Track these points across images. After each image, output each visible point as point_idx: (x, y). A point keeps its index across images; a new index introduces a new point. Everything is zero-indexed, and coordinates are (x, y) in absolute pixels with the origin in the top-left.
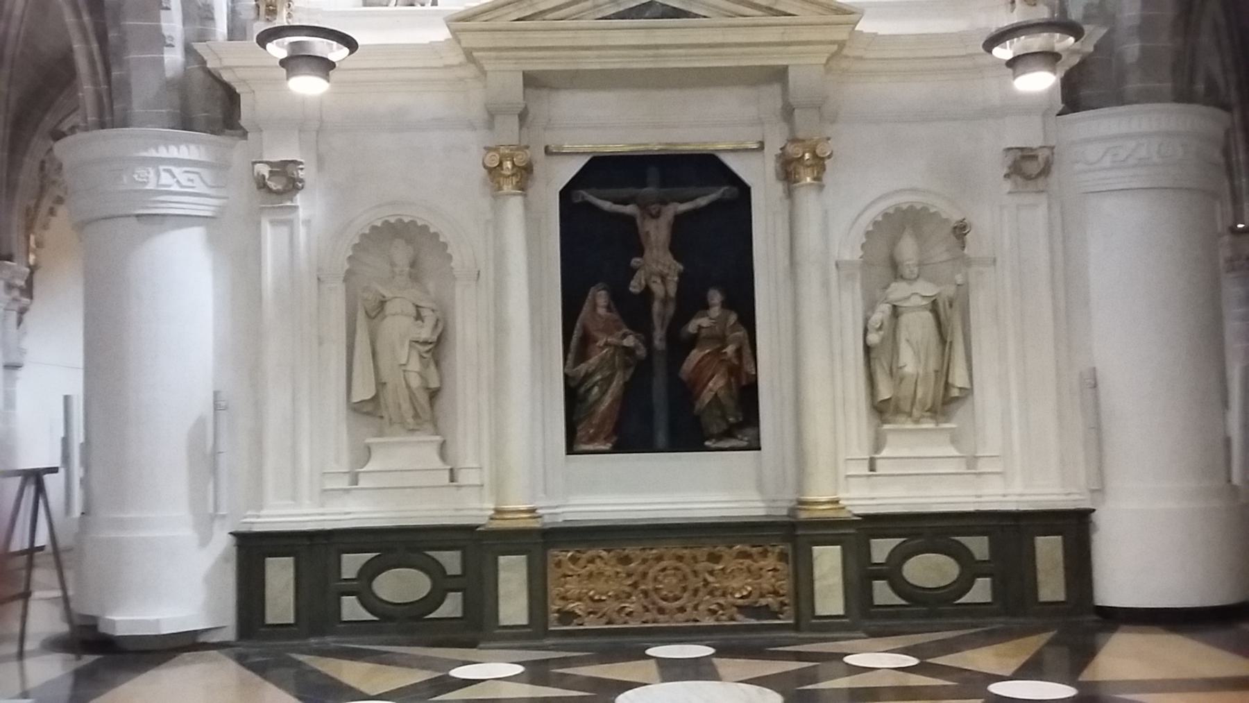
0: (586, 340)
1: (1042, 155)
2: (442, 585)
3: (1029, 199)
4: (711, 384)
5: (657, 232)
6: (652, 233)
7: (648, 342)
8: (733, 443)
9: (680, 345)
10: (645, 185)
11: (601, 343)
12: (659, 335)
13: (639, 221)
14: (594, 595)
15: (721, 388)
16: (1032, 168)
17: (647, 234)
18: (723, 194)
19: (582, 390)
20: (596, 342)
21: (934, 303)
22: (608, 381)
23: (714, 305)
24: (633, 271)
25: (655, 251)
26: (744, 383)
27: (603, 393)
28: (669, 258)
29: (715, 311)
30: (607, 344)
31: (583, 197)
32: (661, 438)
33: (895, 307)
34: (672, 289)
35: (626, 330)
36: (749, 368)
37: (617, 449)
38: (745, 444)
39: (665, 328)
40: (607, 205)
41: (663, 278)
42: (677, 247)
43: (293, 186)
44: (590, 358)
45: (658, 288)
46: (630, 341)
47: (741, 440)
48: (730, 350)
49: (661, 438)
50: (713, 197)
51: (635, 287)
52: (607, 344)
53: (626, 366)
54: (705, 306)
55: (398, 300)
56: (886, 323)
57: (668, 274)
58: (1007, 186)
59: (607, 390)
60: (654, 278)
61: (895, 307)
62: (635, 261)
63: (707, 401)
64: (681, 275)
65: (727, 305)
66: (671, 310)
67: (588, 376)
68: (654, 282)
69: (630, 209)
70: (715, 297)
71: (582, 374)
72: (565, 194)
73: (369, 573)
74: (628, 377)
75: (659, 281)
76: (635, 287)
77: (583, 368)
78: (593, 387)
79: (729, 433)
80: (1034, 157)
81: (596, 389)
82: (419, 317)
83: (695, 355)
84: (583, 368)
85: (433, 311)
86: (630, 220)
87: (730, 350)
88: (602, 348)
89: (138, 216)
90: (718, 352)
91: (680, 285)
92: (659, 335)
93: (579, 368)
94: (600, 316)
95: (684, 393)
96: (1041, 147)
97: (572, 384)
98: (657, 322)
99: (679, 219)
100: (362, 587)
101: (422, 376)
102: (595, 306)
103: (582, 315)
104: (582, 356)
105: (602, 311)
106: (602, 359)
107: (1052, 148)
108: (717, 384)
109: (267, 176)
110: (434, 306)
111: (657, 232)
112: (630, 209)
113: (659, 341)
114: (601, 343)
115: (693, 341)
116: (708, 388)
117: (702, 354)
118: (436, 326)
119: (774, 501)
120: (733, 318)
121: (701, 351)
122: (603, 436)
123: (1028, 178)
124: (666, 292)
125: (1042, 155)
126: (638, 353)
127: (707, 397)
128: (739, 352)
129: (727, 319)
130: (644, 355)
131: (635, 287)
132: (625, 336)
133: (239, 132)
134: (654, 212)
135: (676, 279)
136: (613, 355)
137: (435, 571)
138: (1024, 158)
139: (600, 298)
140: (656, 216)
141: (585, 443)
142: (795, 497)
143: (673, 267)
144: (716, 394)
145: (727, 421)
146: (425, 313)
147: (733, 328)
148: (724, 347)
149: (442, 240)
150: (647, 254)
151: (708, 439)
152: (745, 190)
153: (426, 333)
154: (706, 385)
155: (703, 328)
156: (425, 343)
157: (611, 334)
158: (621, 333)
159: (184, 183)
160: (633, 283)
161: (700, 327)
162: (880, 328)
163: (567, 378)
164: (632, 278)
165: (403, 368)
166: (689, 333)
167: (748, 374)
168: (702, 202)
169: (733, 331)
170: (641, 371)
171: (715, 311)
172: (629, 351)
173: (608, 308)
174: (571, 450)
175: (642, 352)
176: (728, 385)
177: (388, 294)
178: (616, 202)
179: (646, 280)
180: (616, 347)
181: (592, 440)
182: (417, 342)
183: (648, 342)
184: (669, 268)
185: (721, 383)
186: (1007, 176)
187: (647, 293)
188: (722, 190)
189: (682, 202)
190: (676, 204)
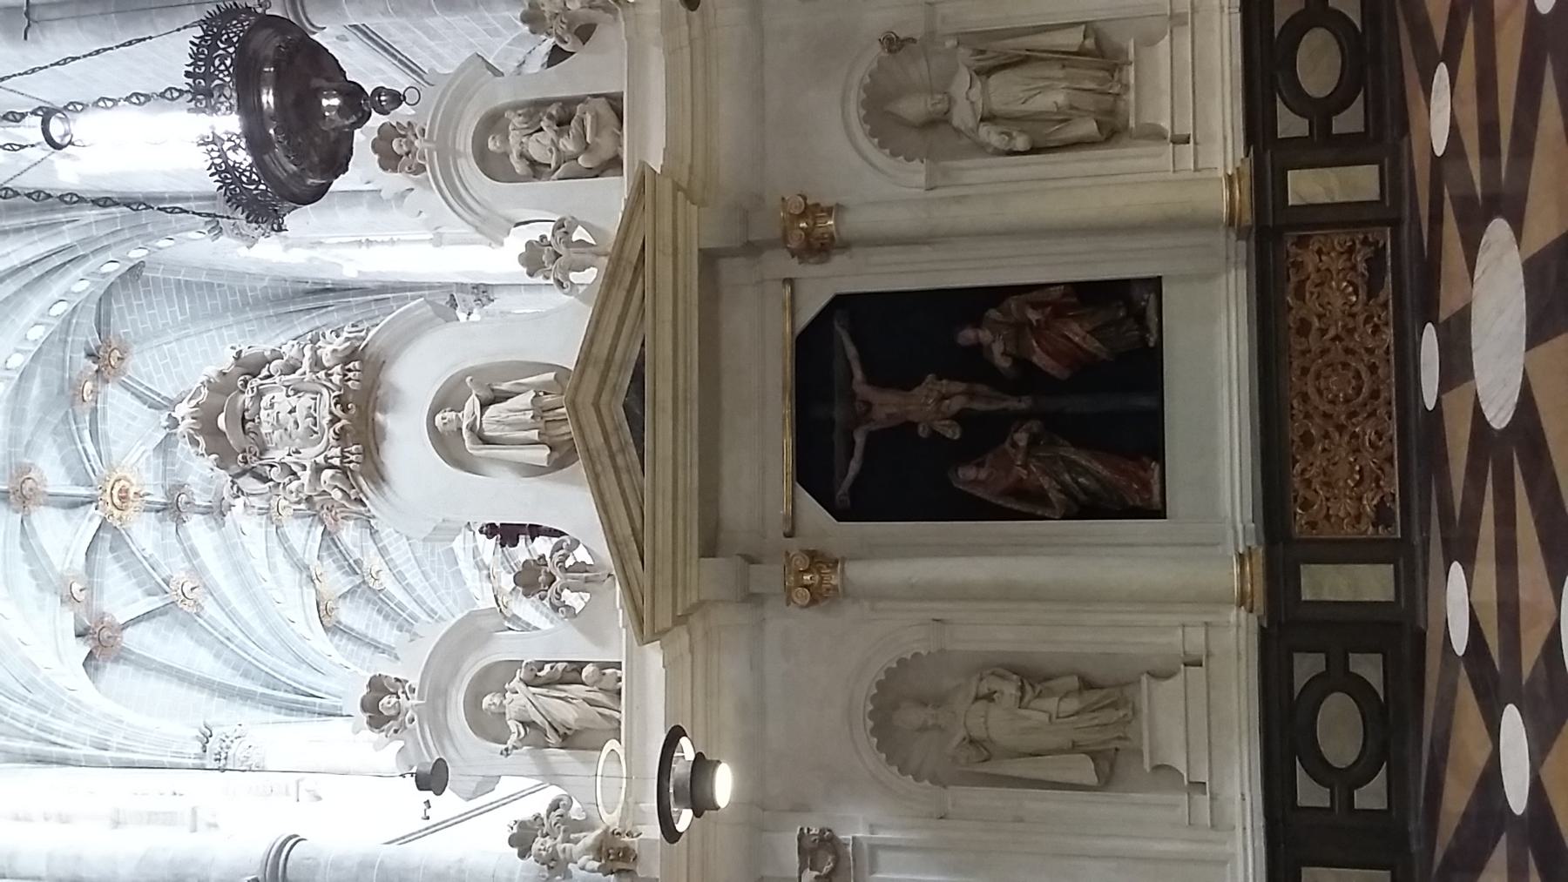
4: (1077, 339)
5: (887, 405)
9: (1026, 377)
14: (1353, 480)
15: (1081, 326)
17: (889, 416)
18: (843, 327)
19: (1082, 497)
22: (1071, 466)
24: (935, 434)
27: (1086, 472)
30: (1025, 466)
31: (845, 495)
34: (959, 386)
40: (854, 466)
42: (906, 382)
44: (1041, 487)
45: (956, 404)
46: (1022, 438)
47: (1147, 301)
48: (1033, 316)
59: (1082, 466)
60: (943, 408)
62: (922, 432)
63: (1097, 344)
66: (982, 388)
67: (1064, 489)
69: (860, 439)
71: (1063, 497)
76: (953, 433)
78: (1077, 483)
81: (1081, 480)
82: (989, 697)
83: (1040, 359)
84: (1054, 495)
85: (981, 679)
86: (871, 438)
87: (1033, 316)
88: (1030, 472)
90: (1037, 330)
91: (951, 378)
95: (1086, 371)
97: (1076, 509)
99: (872, 379)
101: (1067, 694)
102: (976, 482)
105: (983, 475)
106: (1045, 473)
108: (1076, 332)
111: (887, 405)
112: (860, 439)
113: (1023, 404)
119: (1227, 258)
122: (1142, 473)
129: (996, 322)
131: (953, 433)
132: (1014, 445)
136: (1039, 459)
139: (967, 474)
140: (869, 405)
141: (1150, 491)
142: (1222, 232)
144: (1091, 333)
150: (912, 418)
153: (1010, 689)
156: (1022, 689)
160: (949, 435)
161: (1004, 354)
168: (851, 351)
170: (1057, 427)
173: (980, 465)
174: (1160, 514)
175: (1035, 425)
177: (962, 733)
178: (851, 455)
181: (1146, 486)
182: (1021, 699)
185: (1075, 327)
187: (960, 417)
189: (851, 376)
190: (854, 382)
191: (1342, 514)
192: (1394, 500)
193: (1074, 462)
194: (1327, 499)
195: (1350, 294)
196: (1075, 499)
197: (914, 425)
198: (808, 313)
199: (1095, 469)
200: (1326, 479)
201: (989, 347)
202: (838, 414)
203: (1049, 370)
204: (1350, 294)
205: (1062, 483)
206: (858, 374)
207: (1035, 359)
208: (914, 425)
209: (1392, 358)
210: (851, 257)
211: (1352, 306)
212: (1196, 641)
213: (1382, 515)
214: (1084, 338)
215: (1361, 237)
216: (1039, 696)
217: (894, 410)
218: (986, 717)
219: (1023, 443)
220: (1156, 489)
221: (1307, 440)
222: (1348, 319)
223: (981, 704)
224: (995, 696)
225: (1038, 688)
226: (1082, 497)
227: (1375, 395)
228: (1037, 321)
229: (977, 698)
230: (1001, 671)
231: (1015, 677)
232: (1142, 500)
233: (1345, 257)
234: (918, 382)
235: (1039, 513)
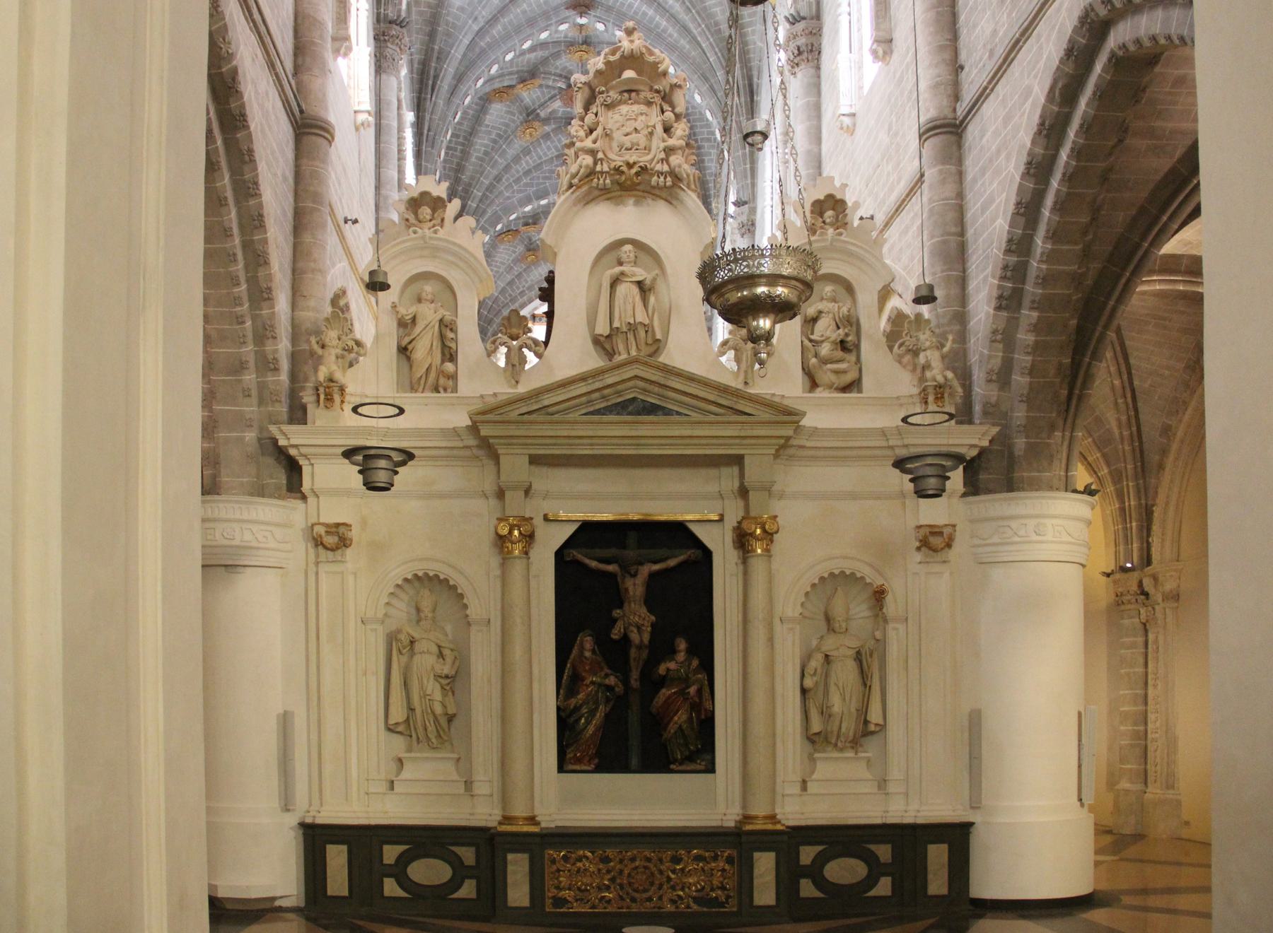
0: (576, 679)
1: (946, 531)
2: (460, 872)
3: (937, 568)
4: (676, 718)
5: (635, 587)
6: (631, 589)
7: (625, 681)
9: (653, 683)
10: (625, 547)
11: (588, 682)
12: (635, 675)
13: (619, 579)
15: (685, 722)
16: (935, 541)
17: (627, 590)
19: (572, 719)
20: (583, 680)
21: (858, 653)
22: (592, 713)
23: (680, 651)
24: (615, 621)
25: (633, 605)
26: (703, 717)
27: (588, 723)
28: (644, 611)
29: (681, 656)
30: (593, 683)
31: (574, 556)
32: (634, 762)
33: (827, 656)
34: (646, 638)
35: (609, 671)
36: (707, 705)
37: (599, 769)
38: (703, 768)
40: (594, 564)
41: (639, 628)
42: (650, 601)
43: (344, 543)
45: (635, 636)
46: (612, 680)
48: (692, 690)
49: (634, 762)
50: (682, 558)
53: (608, 700)
54: (673, 651)
55: (424, 641)
56: (819, 671)
57: (643, 625)
58: (918, 557)
61: (827, 656)
62: (617, 613)
63: (672, 731)
64: (653, 625)
65: (691, 652)
66: (645, 654)
67: (577, 709)
69: (611, 568)
70: (682, 645)
71: (572, 707)
72: (559, 554)
73: (404, 861)
75: (636, 631)
76: (616, 634)
77: (573, 702)
79: (690, 758)
80: (941, 534)
81: (583, 721)
82: (441, 655)
83: (665, 693)
84: (573, 702)
85: (452, 650)
86: (612, 576)
87: (692, 690)
88: (587, 686)
89: (226, 566)
90: (683, 693)
91: (653, 634)
92: (635, 675)
94: (586, 658)
95: (655, 723)
96: (946, 525)
97: (563, 714)
98: (632, 663)
99: (653, 576)
100: (399, 871)
102: (582, 648)
103: (572, 656)
105: (588, 654)
106: (588, 695)
107: (954, 526)
108: (681, 717)
109: (323, 534)
110: (452, 646)
111: (635, 587)
112: (611, 568)
113: (634, 683)
115: (662, 682)
118: (454, 663)
120: (695, 663)
122: (587, 758)
123: (935, 551)
125: (946, 531)
127: (672, 728)
128: (699, 691)
129: (690, 664)
131: (616, 634)
132: (607, 676)
133: (299, 495)
134: (632, 572)
135: (649, 629)
136: (597, 692)
137: (456, 862)
138: (933, 534)
139: (587, 643)
141: (575, 764)
142: (741, 812)
143: (647, 619)
144: (680, 726)
145: (689, 748)
146: (446, 652)
147: (696, 671)
148: (688, 687)
149: (459, 591)
150: (626, 605)
151: (673, 763)
152: (708, 554)
154: (672, 718)
156: (447, 677)
157: (595, 674)
158: (603, 674)
159: (260, 539)
160: (615, 631)
161: (668, 670)
162: (815, 674)
163: (558, 709)
164: (613, 627)
165: (428, 697)
166: (660, 675)
167: (706, 710)
168: (672, 563)
169: (694, 675)
170: (619, 705)
171: (681, 656)
172: (609, 688)
173: (593, 651)
174: (561, 769)
176: (690, 719)
177: (416, 635)
178: (601, 561)
179: (625, 629)
180: (600, 685)
181: (578, 761)
183: (625, 681)
184: (644, 619)
185: (684, 717)
186: (918, 549)
187: (625, 638)
188: (689, 553)
189: (655, 562)
191: (561, 879)
192: (569, 908)
193: (595, 715)
194: (569, 871)
195: (696, 887)
196: (570, 716)
197: (621, 606)
198: (698, 531)
199: (591, 728)
200: (582, 870)
201: (673, 659)
202: (631, 553)
203: (656, 700)
204: (696, 887)
205: (581, 706)
206: (656, 567)
207: (664, 690)
208: (621, 606)
209: (656, 910)
210: (736, 564)
211: (689, 888)
212: (481, 788)
213: (559, 902)
214: (676, 723)
215: (732, 894)
216: (442, 687)
217: (631, 593)
218: (429, 652)
219: (607, 681)
220: (577, 767)
221: (605, 860)
222: (680, 886)
223: (435, 649)
224: (441, 660)
225: (448, 688)
226: (572, 719)
227: (633, 900)
228: (689, 693)
229: (439, 647)
230: (457, 663)
231: (453, 673)
232: (570, 759)
233: (720, 885)
234: (650, 610)
235: (562, 691)
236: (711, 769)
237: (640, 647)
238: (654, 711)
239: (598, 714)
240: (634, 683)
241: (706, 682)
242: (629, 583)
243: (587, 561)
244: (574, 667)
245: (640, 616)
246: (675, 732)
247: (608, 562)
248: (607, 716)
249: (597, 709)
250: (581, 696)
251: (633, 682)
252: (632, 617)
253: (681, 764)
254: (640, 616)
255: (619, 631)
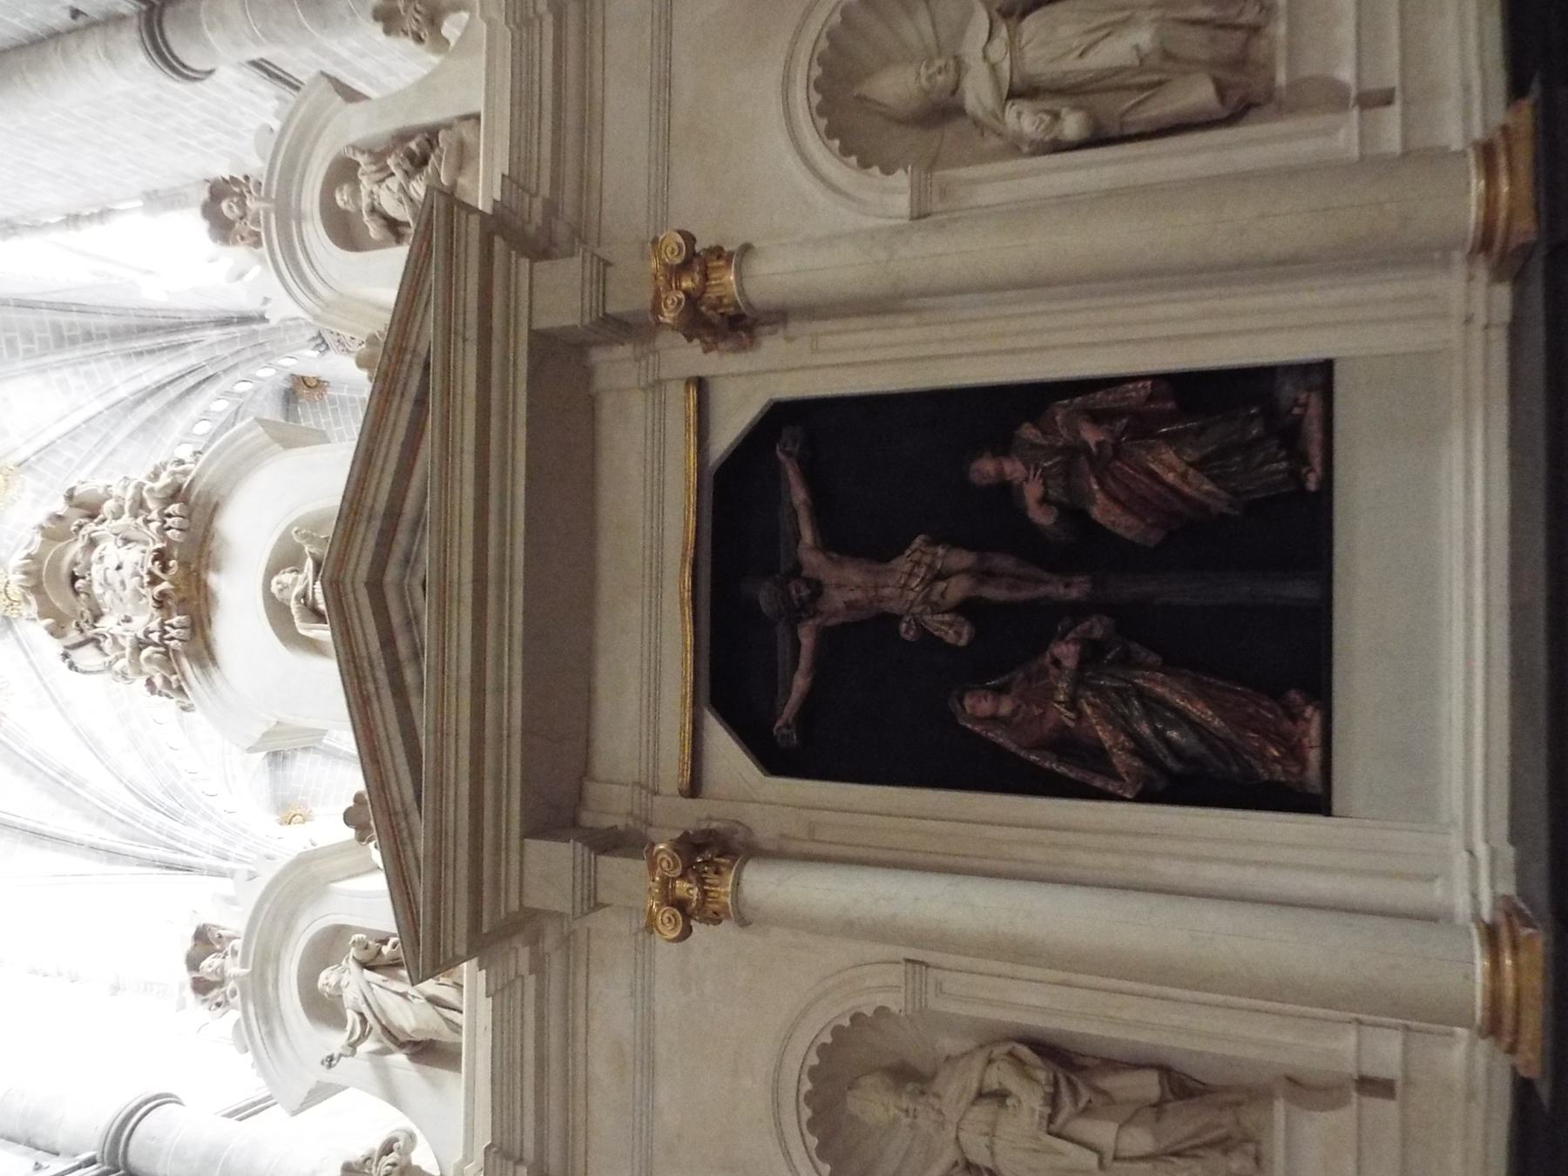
4: (1170, 477)
7: (1078, 611)
8: (1313, 429)
11: (1068, 717)
13: (832, 622)
15: (1178, 453)
17: (850, 605)
19: (1171, 763)
22: (1154, 706)
23: (1000, 472)
25: (887, 592)
27: (1183, 718)
28: (902, 564)
29: (1013, 469)
30: (1072, 704)
34: (962, 559)
36: (1137, 392)
39: (1046, 576)
40: (800, 683)
41: (941, 576)
44: (1099, 739)
45: (957, 589)
46: (1067, 652)
51: (958, 634)
52: (1072, 704)
53: (1126, 661)
57: (930, 567)
60: (935, 597)
62: (906, 631)
63: (1208, 487)
64: (935, 542)
65: (1004, 446)
67: (1141, 749)
68: (943, 595)
69: (807, 639)
70: (985, 468)
74: (1154, 659)
75: (941, 585)
76: (957, 634)
78: (1168, 743)
81: (1173, 734)
83: (1102, 510)
84: (1122, 760)
88: (1080, 715)
90: (1101, 462)
91: (955, 542)
93: (1121, 769)
98: (1024, 594)
104: (1097, 757)
106: (1106, 718)
112: (807, 639)
113: (1076, 590)
114: (1068, 717)
115: (1074, 515)
116: (1178, 483)
117: (1099, 496)
120: (1028, 432)
121: (1093, 501)
124: (966, 571)
126: (1098, 633)
127: (1201, 487)
128: (1098, 417)
129: (1034, 446)
130: (1106, 620)
131: (957, 634)
132: (1057, 662)
135: (941, 551)
136: (1099, 692)
143: (917, 556)
144: (1199, 465)
148: (1085, 448)
150: (894, 607)
154: (1172, 489)
155: (1046, 494)
158: (1053, 671)
161: (1044, 500)
163: (1143, 798)
164: (940, 639)
167: (1150, 398)
171: (1013, 469)
172: (1092, 653)
180: (1079, 681)
183: (1078, 611)
185: (1169, 455)
187: (967, 608)
189: (797, 536)
193: (1162, 702)
201: (1020, 488)
203: (1120, 531)
205: (1134, 736)
206: (807, 535)
207: (1096, 513)
208: (891, 620)
214: (1184, 476)
219: (1070, 663)
228: (1099, 444)
236: (1320, 375)
237: (984, 575)
238: (1155, 537)
239: (1159, 690)
240: (1076, 590)
241: (1078, 400)
242: (836, 600)
243: (795, 696)
244: (1036, 746)
245: (911, 575)
246: (1213, 479)
247: (797, 645)
248: (1173, 663)
249: (1141, 694)
250: (1104, 735)
251: (1074, 593)
252: (912, 595)
253: (1304, 459)
254: (911, 575)
255: (951, 625)
